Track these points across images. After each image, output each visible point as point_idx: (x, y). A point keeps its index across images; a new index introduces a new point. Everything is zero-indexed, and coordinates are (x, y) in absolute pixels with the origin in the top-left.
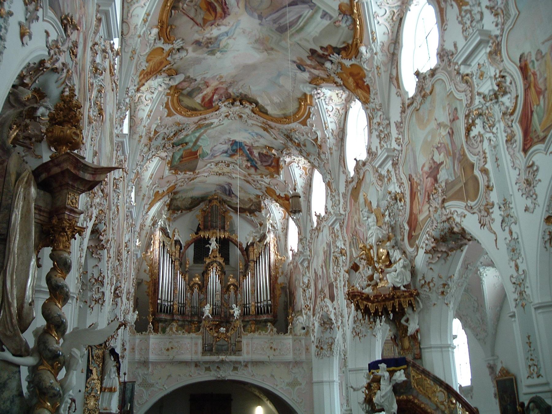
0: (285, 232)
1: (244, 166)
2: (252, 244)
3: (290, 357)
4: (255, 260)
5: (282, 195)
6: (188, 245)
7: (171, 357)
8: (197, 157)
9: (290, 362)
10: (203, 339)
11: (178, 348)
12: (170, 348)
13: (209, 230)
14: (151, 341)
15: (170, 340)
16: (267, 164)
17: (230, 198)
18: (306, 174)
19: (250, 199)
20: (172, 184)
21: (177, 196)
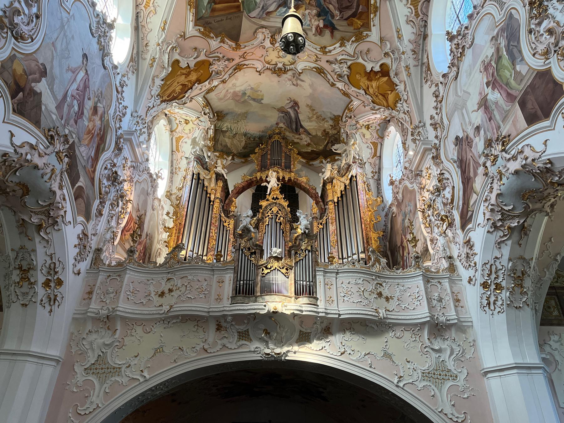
0: (376, 177)
1: (314, 29)
2: (331, 180)
3: (421, 312)
4: (336, 200)
5: (377, 69)
6: (240, 191)
7: (166, 308)
8: (238, 7)
9: (424, 324)
10: (236, 271)
11: (183, 289)
12: (166, 291)
13: (268, 169)
14: (127, 276)
15: (170, 276)
16: (350, 13)
17: (297, 136)
18: (417, 15)
19: (325, 131)
20: (202, 57)
21: (225, 125)
